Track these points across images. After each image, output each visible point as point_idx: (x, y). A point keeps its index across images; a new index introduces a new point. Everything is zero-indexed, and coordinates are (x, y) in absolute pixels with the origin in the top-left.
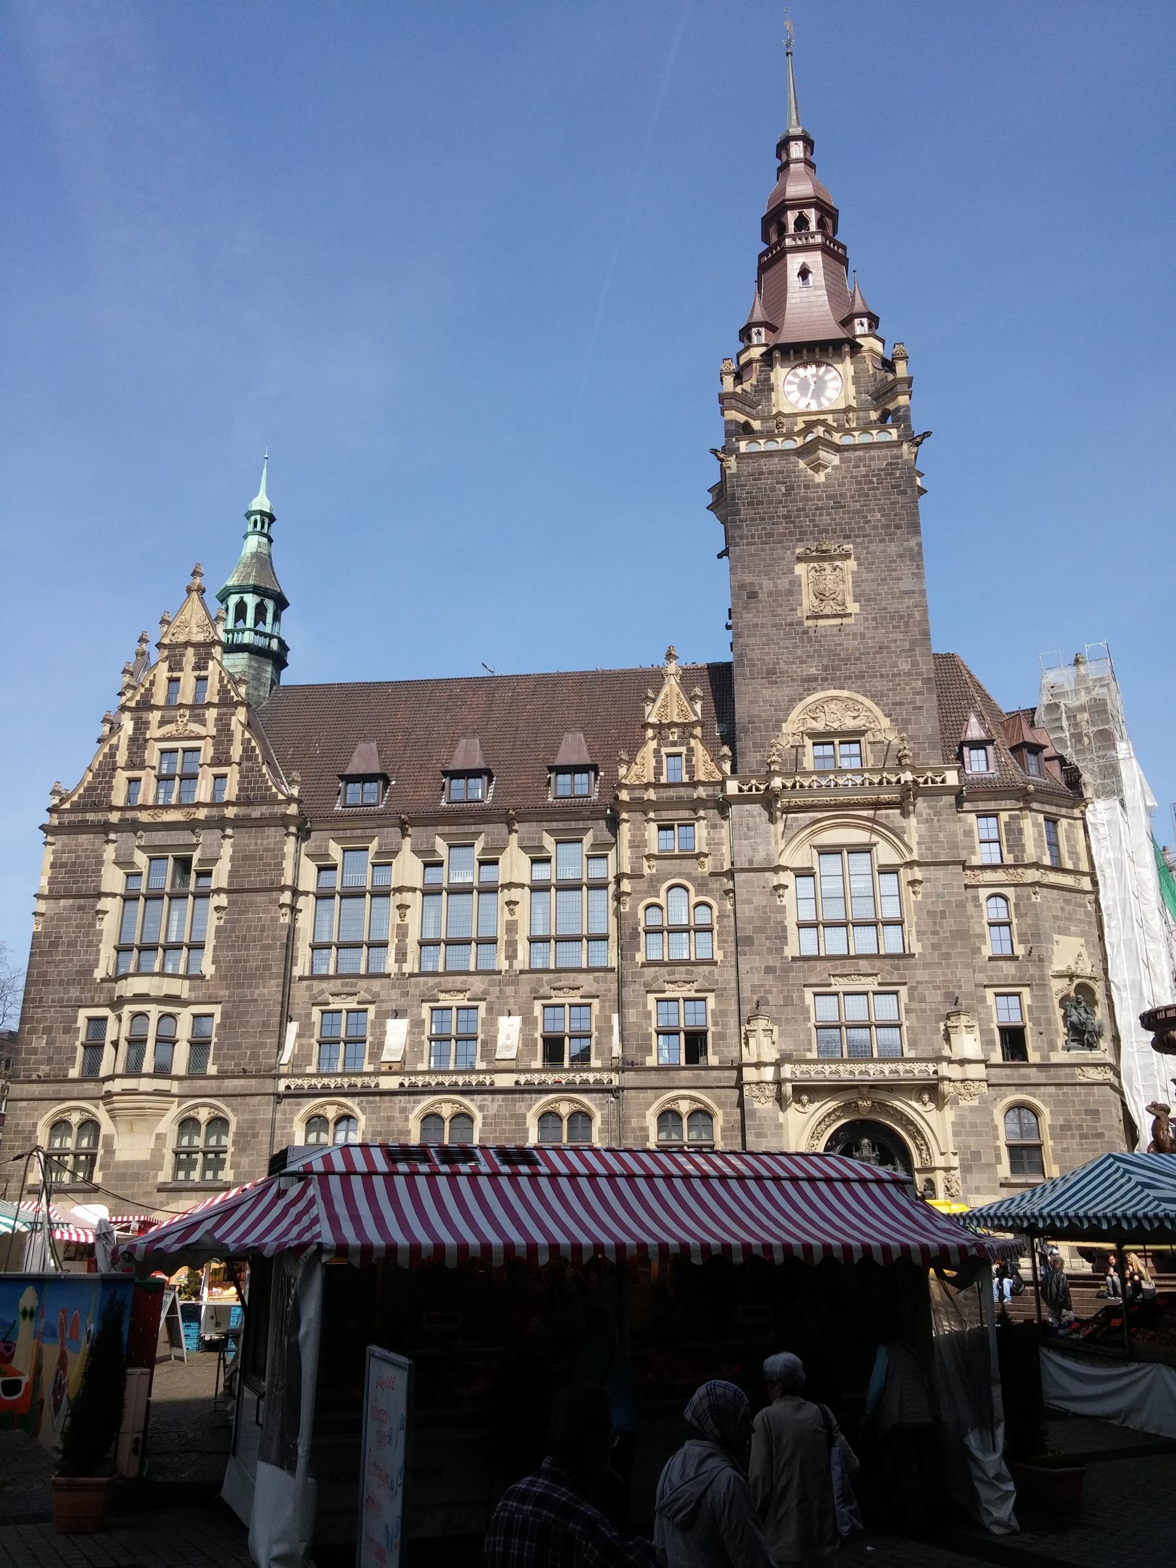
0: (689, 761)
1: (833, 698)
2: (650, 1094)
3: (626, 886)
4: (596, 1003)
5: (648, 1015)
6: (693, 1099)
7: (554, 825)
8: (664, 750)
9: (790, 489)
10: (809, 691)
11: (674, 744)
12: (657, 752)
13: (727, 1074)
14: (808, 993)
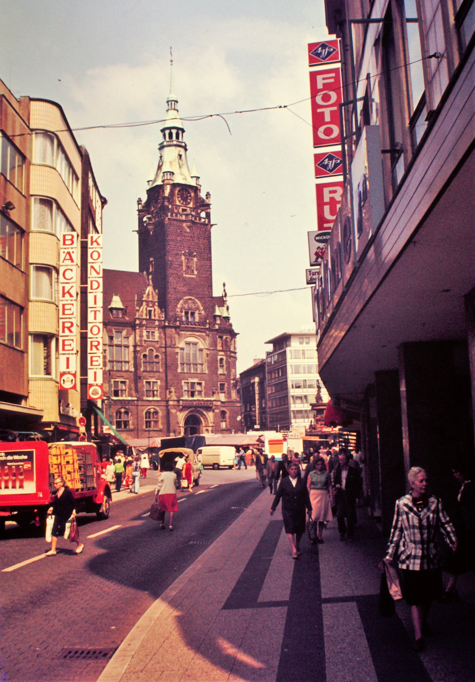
0: (154, 313)
1: (191, 299)
2: (144, 407)
3: (138, 349)
4: (127, 381)
5: (143, 386)
6: (154, 409)
7: (115, 327)
8: (149, 309)
9: (181, 231)
10: (184, 296)
11: (151, 307)
12: (146, 309)
13: (162, 402)
14: (183, 381)
